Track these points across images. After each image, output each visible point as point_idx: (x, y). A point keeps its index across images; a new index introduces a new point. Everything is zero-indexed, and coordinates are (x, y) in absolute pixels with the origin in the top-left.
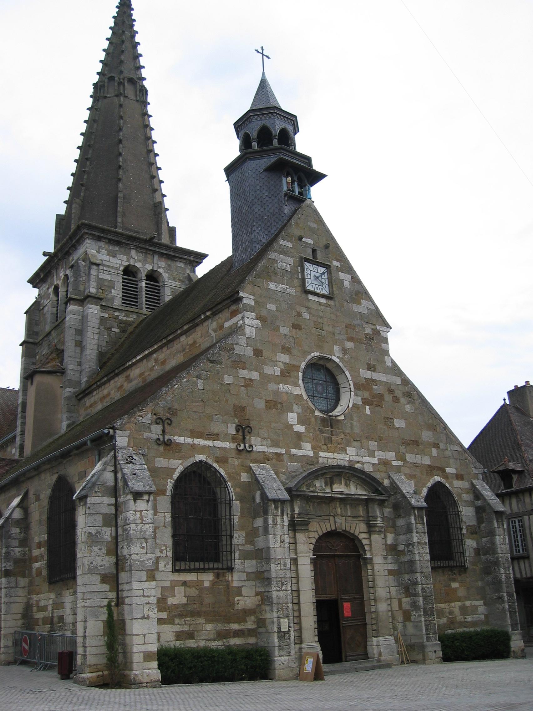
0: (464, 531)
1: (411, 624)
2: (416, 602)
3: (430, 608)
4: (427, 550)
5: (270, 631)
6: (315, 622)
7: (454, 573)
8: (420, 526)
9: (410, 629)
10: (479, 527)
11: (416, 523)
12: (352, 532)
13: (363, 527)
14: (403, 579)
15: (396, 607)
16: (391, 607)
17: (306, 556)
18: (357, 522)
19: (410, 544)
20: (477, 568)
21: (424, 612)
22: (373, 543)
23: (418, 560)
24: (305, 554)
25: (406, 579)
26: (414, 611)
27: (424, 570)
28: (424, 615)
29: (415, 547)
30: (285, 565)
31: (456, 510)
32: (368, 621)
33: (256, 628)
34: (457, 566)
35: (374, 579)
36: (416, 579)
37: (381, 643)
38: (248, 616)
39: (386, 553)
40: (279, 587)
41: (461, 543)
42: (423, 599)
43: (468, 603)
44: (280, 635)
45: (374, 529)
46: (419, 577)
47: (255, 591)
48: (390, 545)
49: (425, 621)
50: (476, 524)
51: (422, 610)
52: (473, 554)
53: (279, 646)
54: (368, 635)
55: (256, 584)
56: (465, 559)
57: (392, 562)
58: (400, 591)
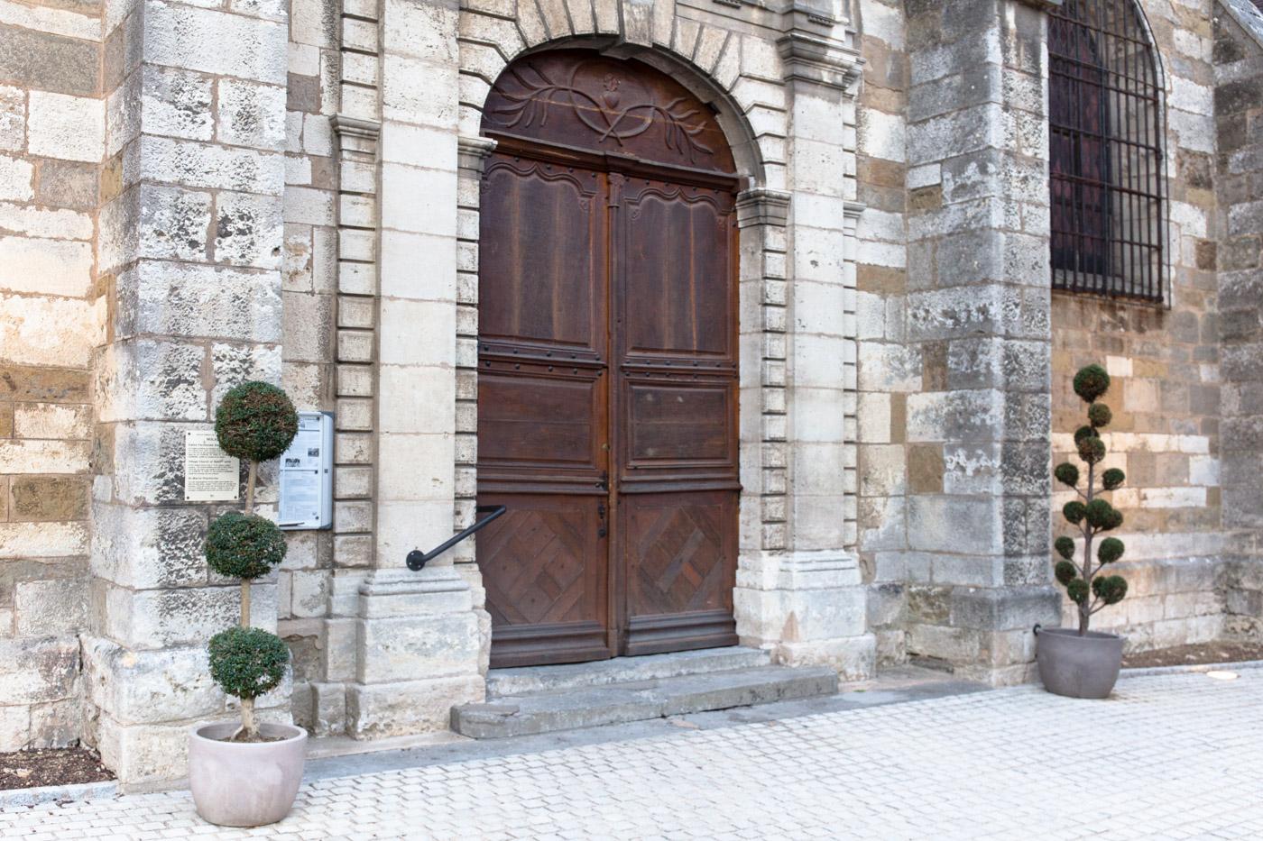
0: (1171, 170)
1: (941, 505)
2: (974, 413)
3: (1033, 441)
4: (1043, 194)
5: (122, 497)
6: (458, 465)
7: (1122, 320)
8: (1019, 82)
9: (934, 522)
10: (1223, 163)
11: (1007, 65)
12: (704, 63)
13: (762, 57)
14: (921, 314)
15: (877, 424)
16: (859, 428)
17: (437, 129)
18: (735, 25)
19: (968, 158)
20: (1199, 315)
21: (1007, 457)
22: (798, 130)
23: (999, 229)
24: (435, 121)
25: (936, 313)
26: (961, 452)
27: (1022, 276)
28: (1005, 472)
29: (991, 168)
30: (247, 119)
31: (1150, 81)
32: (749, 476)
33: (80, 473)
34: (1132, 296)
35: (790, 293)
36: (983, 311)
37: (798, 580)
38: (30, 405)
39: (859, 192)
40: (193, 244)
41: (1154, 209)
42: (1008, 399)
43: (1157, 442)
44: (176, 525)
45: (811, 72)
46: (994, 298)
47: (93, 269)
48: (879, 165)
49: (1008, 496)
50: (1210, 151)
51: (998, 446)
52: (1190, 262)
53: (167, 587)
54: (742, 540)
55: (96, 232)
56: (1165, 275)
57: (881, 235)
58: (902, 363)
